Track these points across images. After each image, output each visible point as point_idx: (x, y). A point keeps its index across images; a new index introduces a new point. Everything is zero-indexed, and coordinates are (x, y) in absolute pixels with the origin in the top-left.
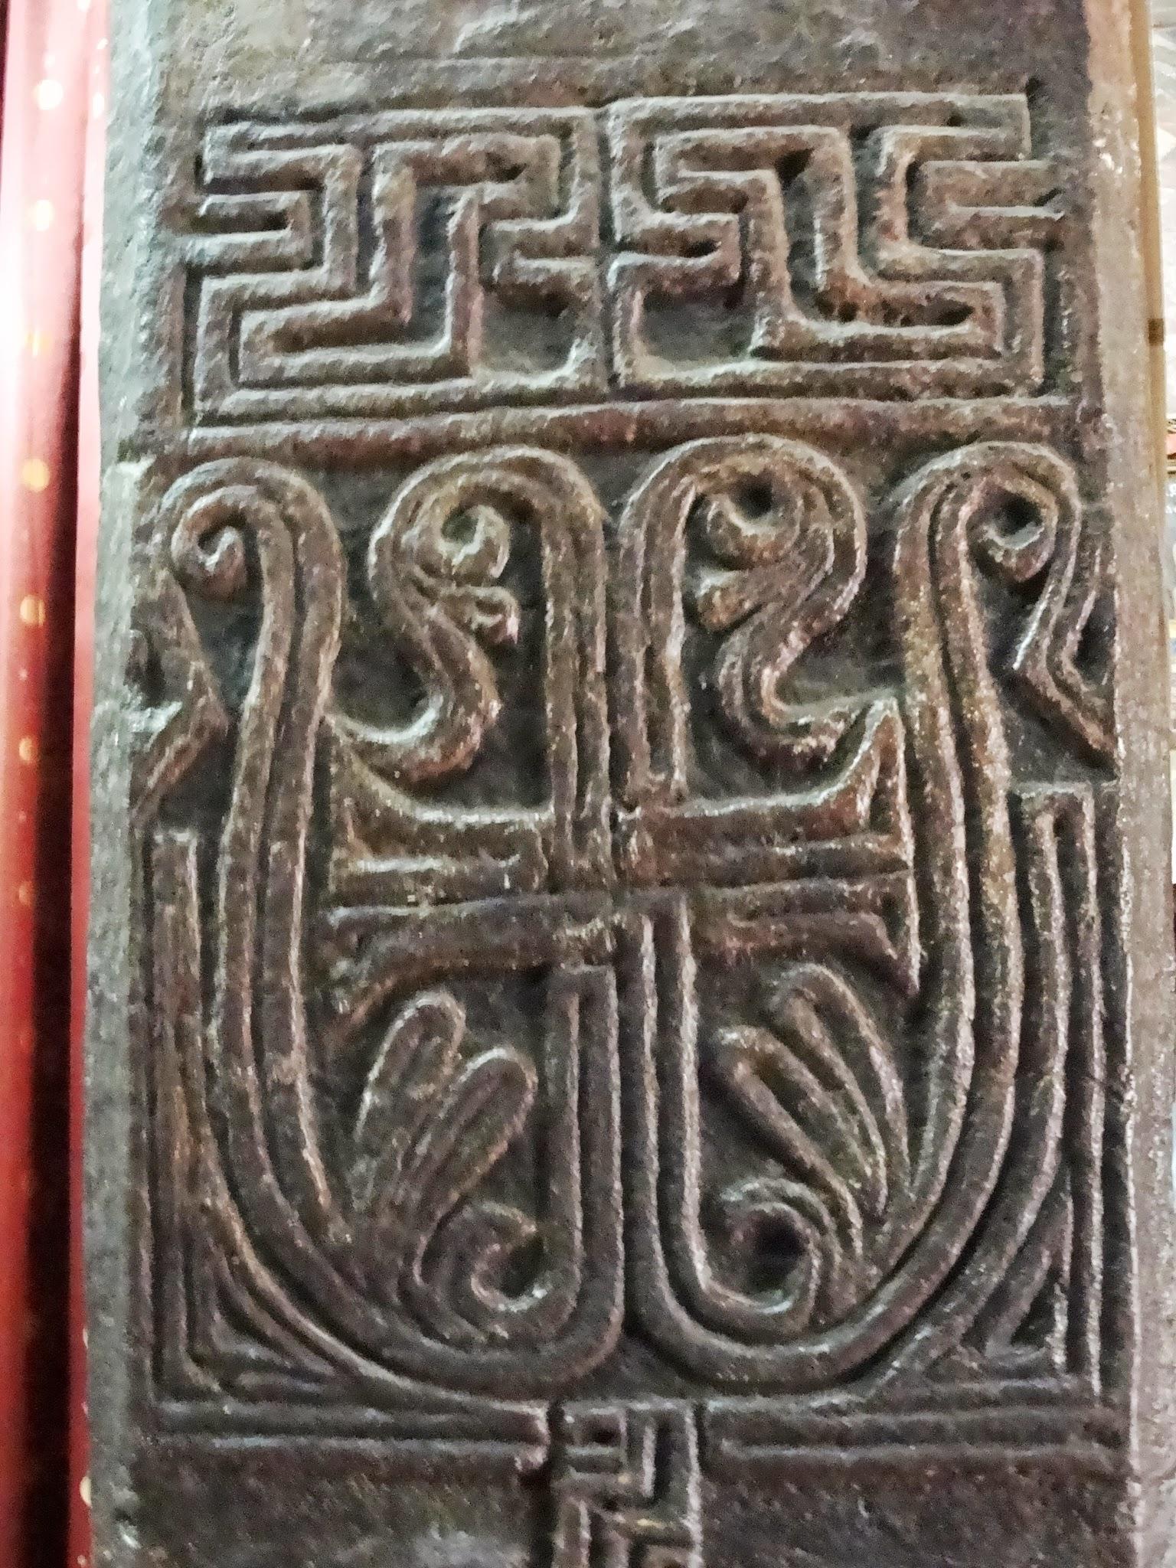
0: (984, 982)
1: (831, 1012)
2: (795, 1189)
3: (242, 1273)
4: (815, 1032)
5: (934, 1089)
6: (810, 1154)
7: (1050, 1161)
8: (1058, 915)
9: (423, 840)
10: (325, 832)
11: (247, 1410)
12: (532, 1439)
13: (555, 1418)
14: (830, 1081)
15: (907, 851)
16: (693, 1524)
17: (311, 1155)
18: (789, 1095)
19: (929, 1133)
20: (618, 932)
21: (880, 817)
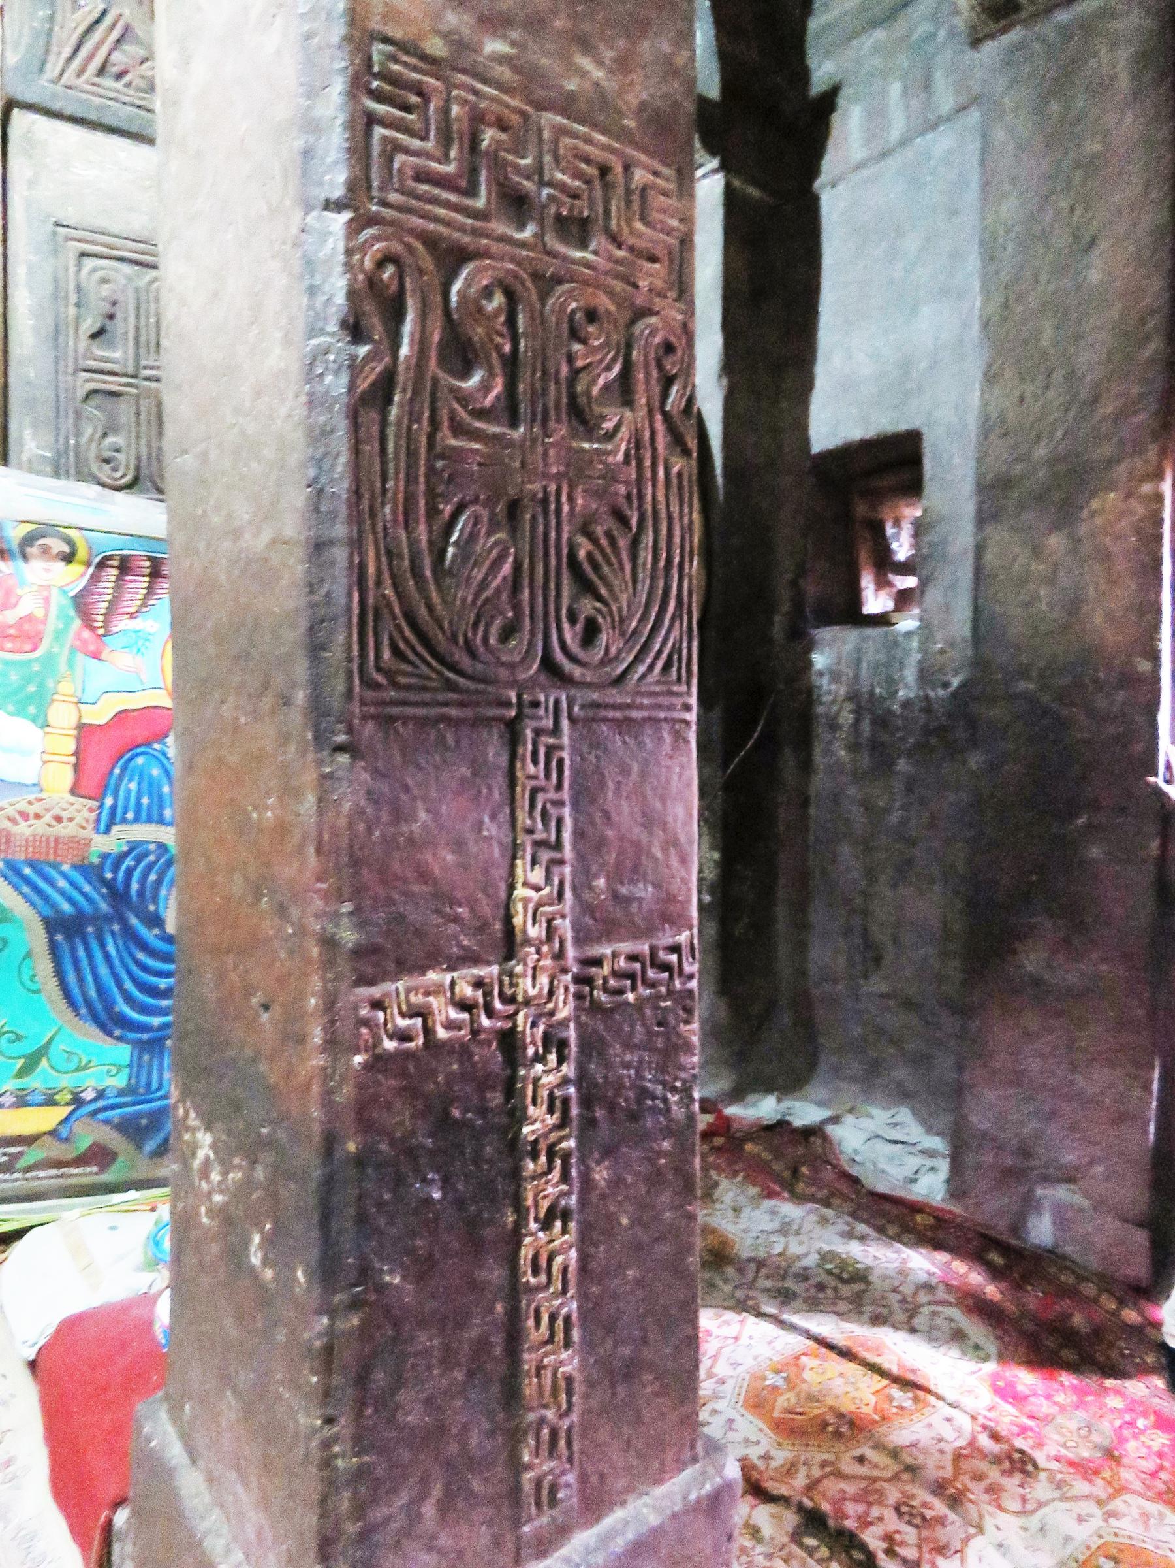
1: (609, 535)
2: (598, 605)
4: (604, 542)
5: (640, 570)
6: (603, 591)
9: (475, 435)
10: (434, 423)
11: (403, 695)
13: (519, 697)
15: (634, 476)
16: (566, 740)
19: (639, 587)
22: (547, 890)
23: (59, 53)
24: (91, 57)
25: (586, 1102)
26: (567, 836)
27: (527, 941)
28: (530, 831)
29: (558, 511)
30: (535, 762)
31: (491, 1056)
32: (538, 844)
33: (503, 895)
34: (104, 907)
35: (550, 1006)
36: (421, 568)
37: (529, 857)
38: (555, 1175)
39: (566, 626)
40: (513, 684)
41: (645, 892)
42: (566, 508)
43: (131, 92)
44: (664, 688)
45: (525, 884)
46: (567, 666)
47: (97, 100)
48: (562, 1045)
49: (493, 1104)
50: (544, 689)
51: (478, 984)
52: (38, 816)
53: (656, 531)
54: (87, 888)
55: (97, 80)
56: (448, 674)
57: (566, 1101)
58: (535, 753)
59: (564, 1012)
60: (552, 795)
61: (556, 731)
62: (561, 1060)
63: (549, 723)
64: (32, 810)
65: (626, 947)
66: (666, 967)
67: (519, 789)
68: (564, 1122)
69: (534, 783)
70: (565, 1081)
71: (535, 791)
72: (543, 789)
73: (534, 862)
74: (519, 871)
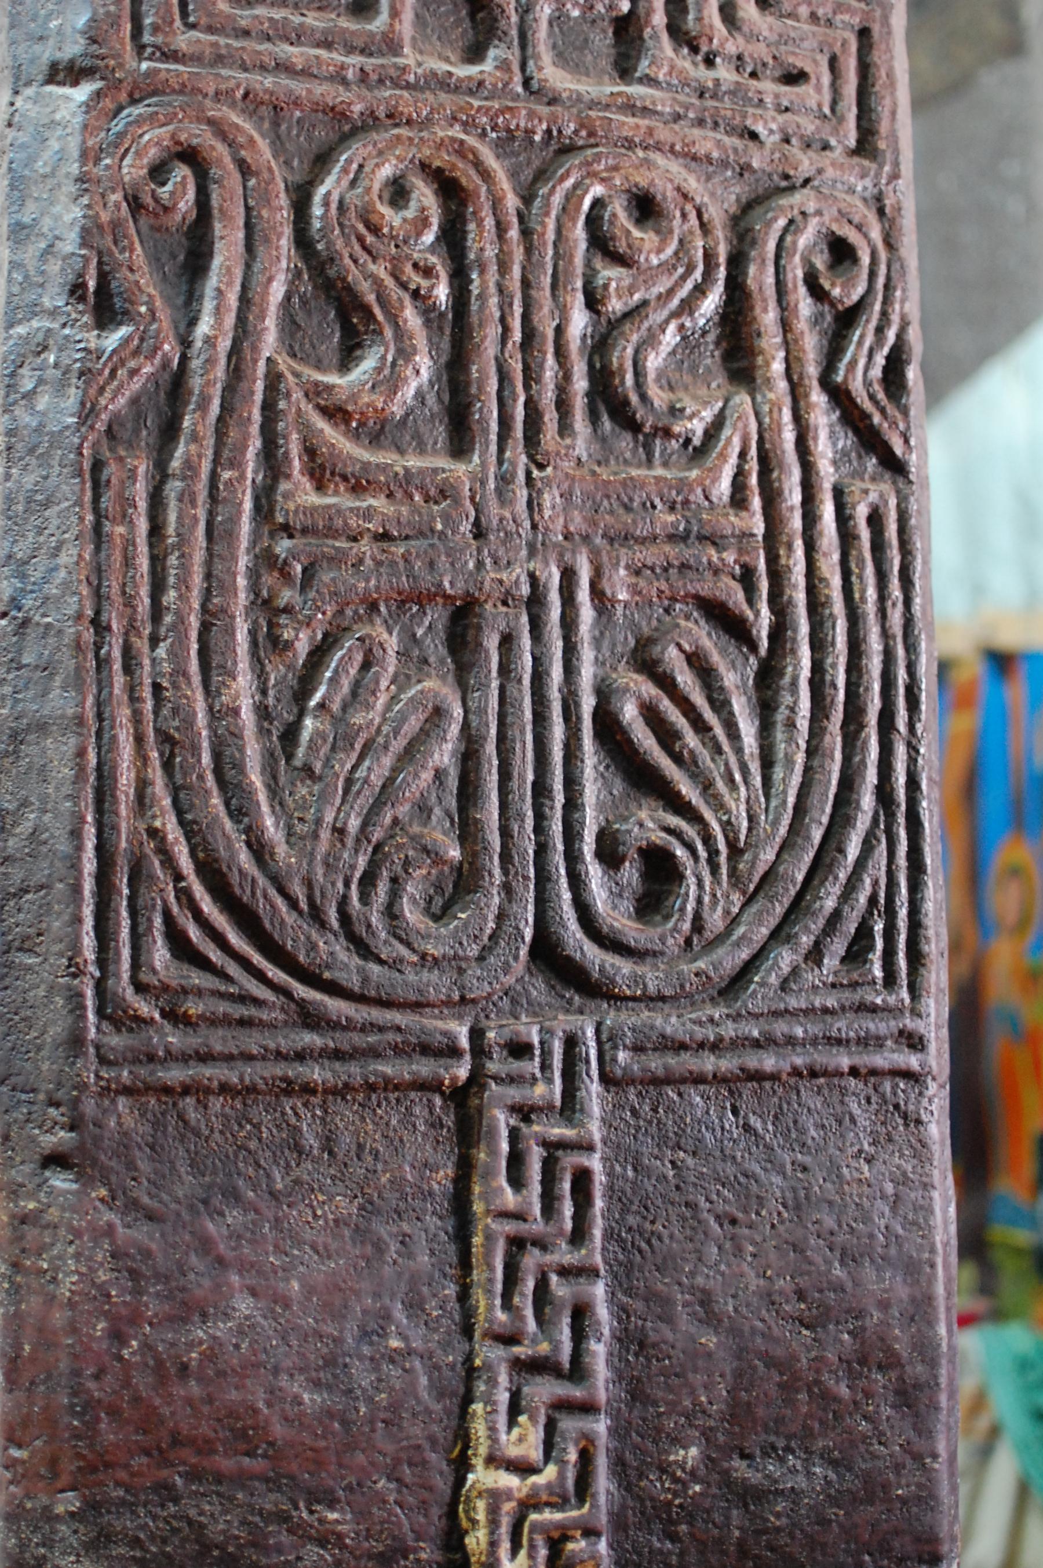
0: (819, 644)
2: (674, 821)
3: (185, 897)
4: (685, 679)
5: (780, 735)
6: (687, 789)
7: (867, 801)
8: (871, 593)
12: (453, 1052)
13: (477, 1034)
14: (700, 726)
15: (759, 527)
16: (595, 1131)
17: (256, 779)
18: (667, 736)
19: (778, 773)
20: (532, 577)
21: (738, 499)
22: (551, 1472)
26: (599, 1350)
28: (509, 1339)
29: (569, 624)
30: (517, 1181)
32: (518, 1365)
33: (442, 1485)
36: (240, 767)
37: (503, 1397)
39: (594, 872)
42: (587, 614)
44: (849, 997)
45: (493, 1461)
46: (592, 955)
50: (535, 1010)
53: (819, 644)
58: (516, 1161)
60: (564, 1255)
67: (477, 1240)
69: (510, 1227)
71: (517, 1244)
72: (542, 1244)
73: (515, 1409)
74: (479, 1429)
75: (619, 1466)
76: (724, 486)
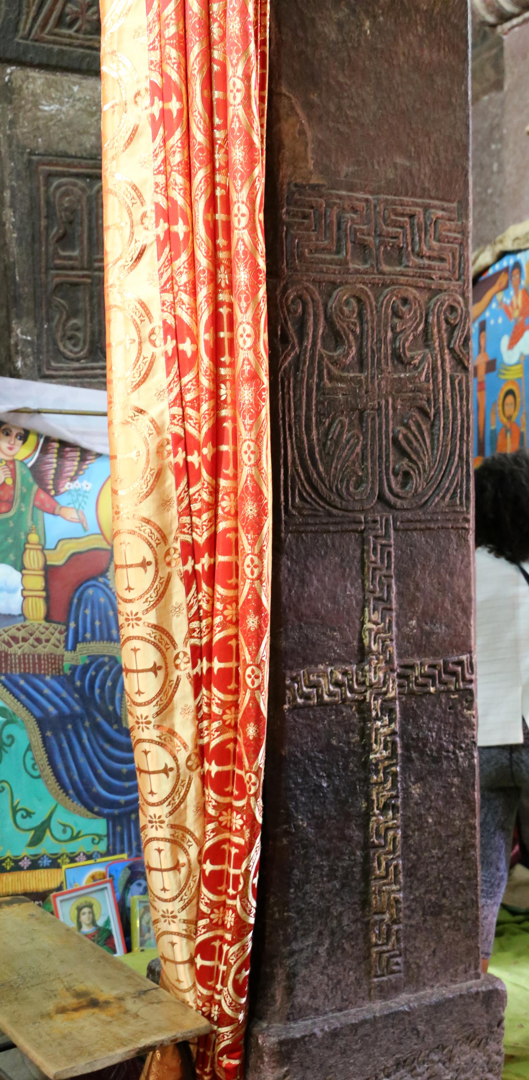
0: (446, 418)
2: (410, 464)
4: (414, 428)
6: (414, 457)
7: (456, 459)
8: (458, 403)
14: (418, 440)
16: (392, 542)
18: (409, 442)
20: (379, 403)
21: (427, 380)
22: (382, 625)
23: (28, 13)
24: (51, 11)
25: (406, 747)
26: (393, 595)
27: (371, 652)
28: (373, 592)
31: (351, 712)
32: (376, 599)
33: (358, 627)
34: (77, 708)
35: (384, 689)
37: (372, 606)
38: (389, 785)
39: (392, 477)
40: (362, 511)
41: (441, 630)
42: (391, 412)
43: (81, 36)
45: (370, 621)
46: (392, 499)
47: (56, 48)
48: (391, 711)
49: (353, 741)
50: (378, 512)
51: (345, 673)
52: (24, 640)
53: (446, 418)
54: (64, 694)
55: (57, 30)
56: (327, 507)
57: (394, 743)
58: (375, 549)
59: (391, 694)
60: (384, 572)
61: (387, 536)
62: (391, 721)
63: (382, 532)
64: (20, 635)
65: (429, 660)
66: (454, 674)
68: (394, 754)
69: (373, 565)
70: (393, 733)
71: (374, 569)
72: (380, 569)
73: (374, 610)
74: (367, 614)
75: (397, 624)
76: (423, 378)
